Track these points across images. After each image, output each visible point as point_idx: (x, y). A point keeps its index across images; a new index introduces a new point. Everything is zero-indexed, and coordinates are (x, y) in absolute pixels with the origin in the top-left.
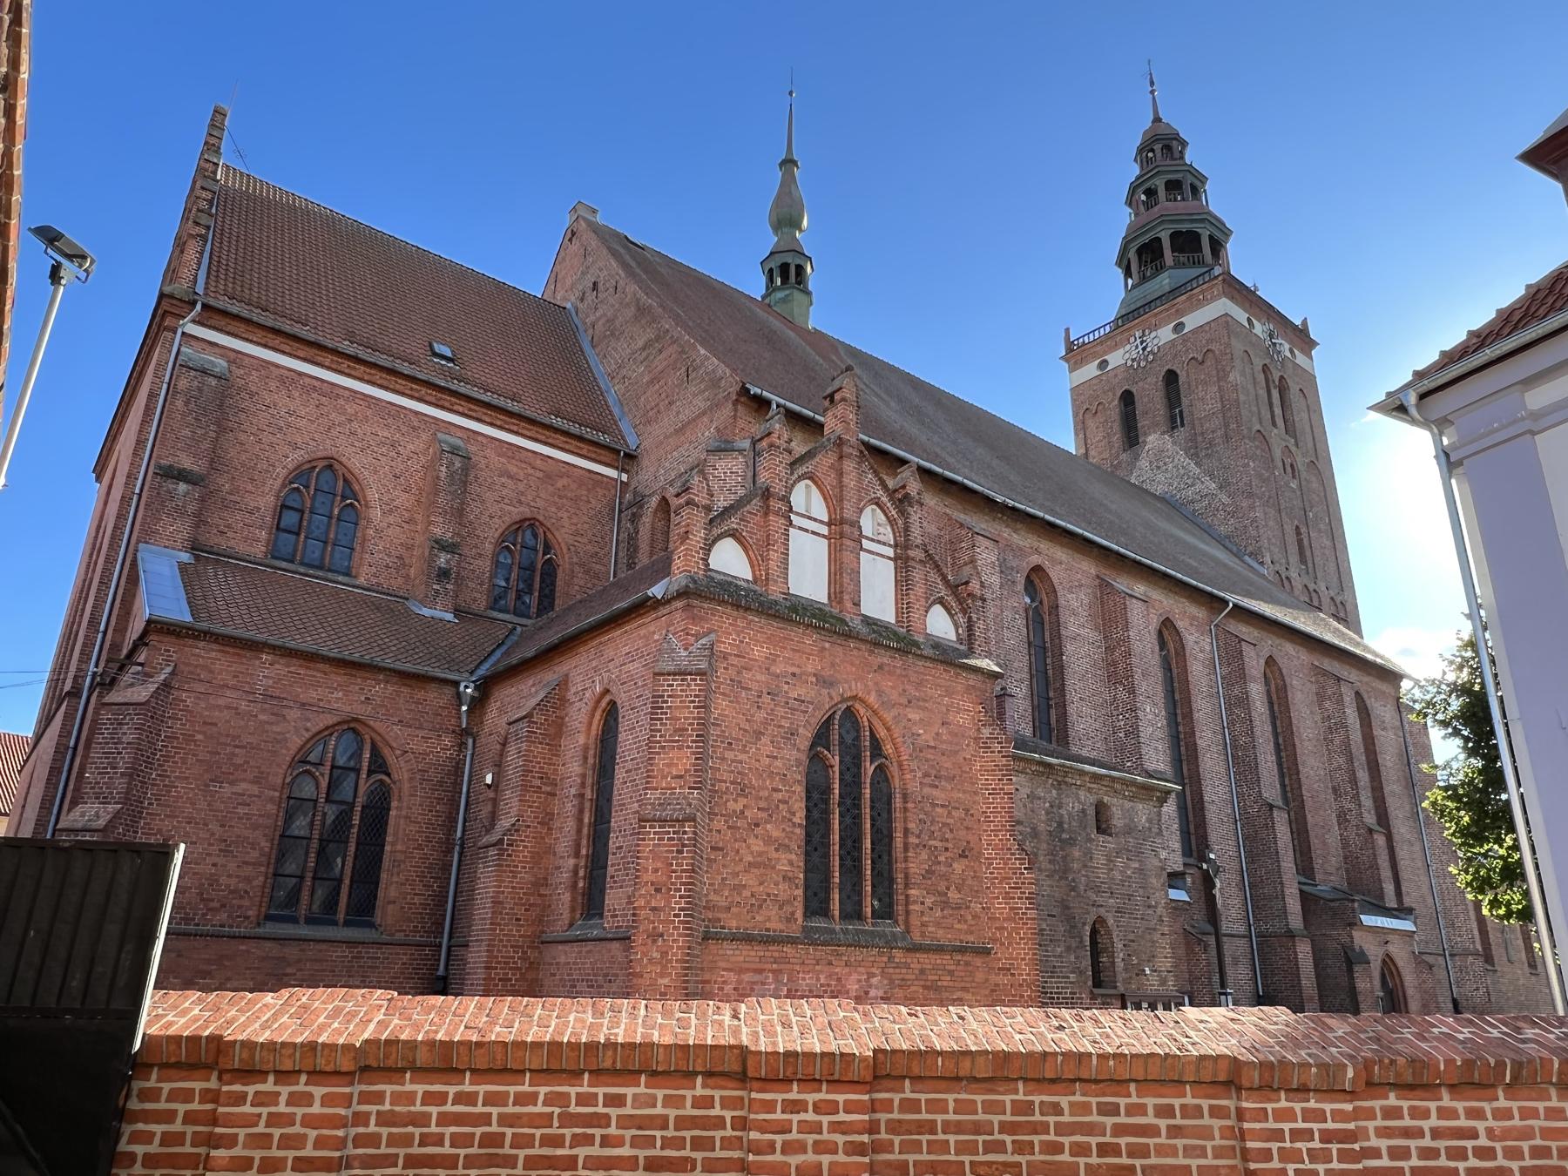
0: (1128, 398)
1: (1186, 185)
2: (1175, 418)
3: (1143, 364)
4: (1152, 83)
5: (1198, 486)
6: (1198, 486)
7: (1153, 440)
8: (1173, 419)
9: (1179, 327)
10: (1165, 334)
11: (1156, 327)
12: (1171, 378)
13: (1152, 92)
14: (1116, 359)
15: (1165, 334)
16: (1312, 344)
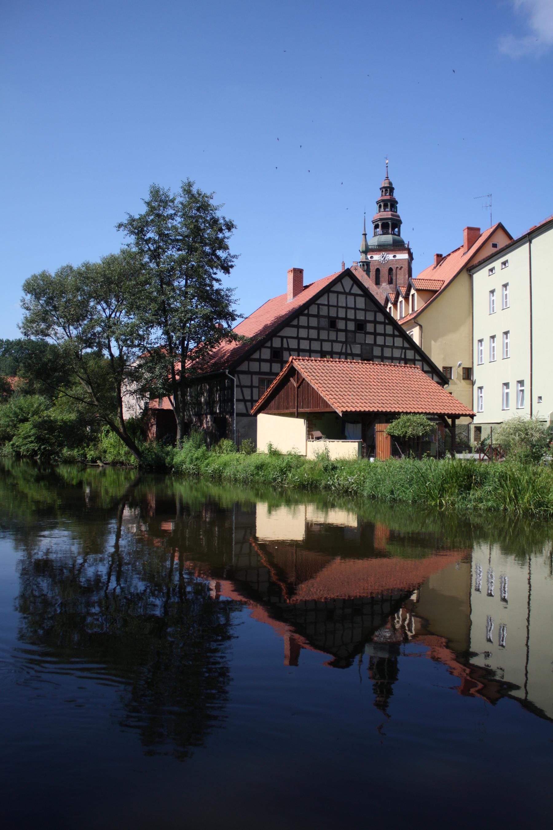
0: (378, 270)
9: (394, 256)
10: (390, 257)
11: (389, 254)
12: (391, 270)
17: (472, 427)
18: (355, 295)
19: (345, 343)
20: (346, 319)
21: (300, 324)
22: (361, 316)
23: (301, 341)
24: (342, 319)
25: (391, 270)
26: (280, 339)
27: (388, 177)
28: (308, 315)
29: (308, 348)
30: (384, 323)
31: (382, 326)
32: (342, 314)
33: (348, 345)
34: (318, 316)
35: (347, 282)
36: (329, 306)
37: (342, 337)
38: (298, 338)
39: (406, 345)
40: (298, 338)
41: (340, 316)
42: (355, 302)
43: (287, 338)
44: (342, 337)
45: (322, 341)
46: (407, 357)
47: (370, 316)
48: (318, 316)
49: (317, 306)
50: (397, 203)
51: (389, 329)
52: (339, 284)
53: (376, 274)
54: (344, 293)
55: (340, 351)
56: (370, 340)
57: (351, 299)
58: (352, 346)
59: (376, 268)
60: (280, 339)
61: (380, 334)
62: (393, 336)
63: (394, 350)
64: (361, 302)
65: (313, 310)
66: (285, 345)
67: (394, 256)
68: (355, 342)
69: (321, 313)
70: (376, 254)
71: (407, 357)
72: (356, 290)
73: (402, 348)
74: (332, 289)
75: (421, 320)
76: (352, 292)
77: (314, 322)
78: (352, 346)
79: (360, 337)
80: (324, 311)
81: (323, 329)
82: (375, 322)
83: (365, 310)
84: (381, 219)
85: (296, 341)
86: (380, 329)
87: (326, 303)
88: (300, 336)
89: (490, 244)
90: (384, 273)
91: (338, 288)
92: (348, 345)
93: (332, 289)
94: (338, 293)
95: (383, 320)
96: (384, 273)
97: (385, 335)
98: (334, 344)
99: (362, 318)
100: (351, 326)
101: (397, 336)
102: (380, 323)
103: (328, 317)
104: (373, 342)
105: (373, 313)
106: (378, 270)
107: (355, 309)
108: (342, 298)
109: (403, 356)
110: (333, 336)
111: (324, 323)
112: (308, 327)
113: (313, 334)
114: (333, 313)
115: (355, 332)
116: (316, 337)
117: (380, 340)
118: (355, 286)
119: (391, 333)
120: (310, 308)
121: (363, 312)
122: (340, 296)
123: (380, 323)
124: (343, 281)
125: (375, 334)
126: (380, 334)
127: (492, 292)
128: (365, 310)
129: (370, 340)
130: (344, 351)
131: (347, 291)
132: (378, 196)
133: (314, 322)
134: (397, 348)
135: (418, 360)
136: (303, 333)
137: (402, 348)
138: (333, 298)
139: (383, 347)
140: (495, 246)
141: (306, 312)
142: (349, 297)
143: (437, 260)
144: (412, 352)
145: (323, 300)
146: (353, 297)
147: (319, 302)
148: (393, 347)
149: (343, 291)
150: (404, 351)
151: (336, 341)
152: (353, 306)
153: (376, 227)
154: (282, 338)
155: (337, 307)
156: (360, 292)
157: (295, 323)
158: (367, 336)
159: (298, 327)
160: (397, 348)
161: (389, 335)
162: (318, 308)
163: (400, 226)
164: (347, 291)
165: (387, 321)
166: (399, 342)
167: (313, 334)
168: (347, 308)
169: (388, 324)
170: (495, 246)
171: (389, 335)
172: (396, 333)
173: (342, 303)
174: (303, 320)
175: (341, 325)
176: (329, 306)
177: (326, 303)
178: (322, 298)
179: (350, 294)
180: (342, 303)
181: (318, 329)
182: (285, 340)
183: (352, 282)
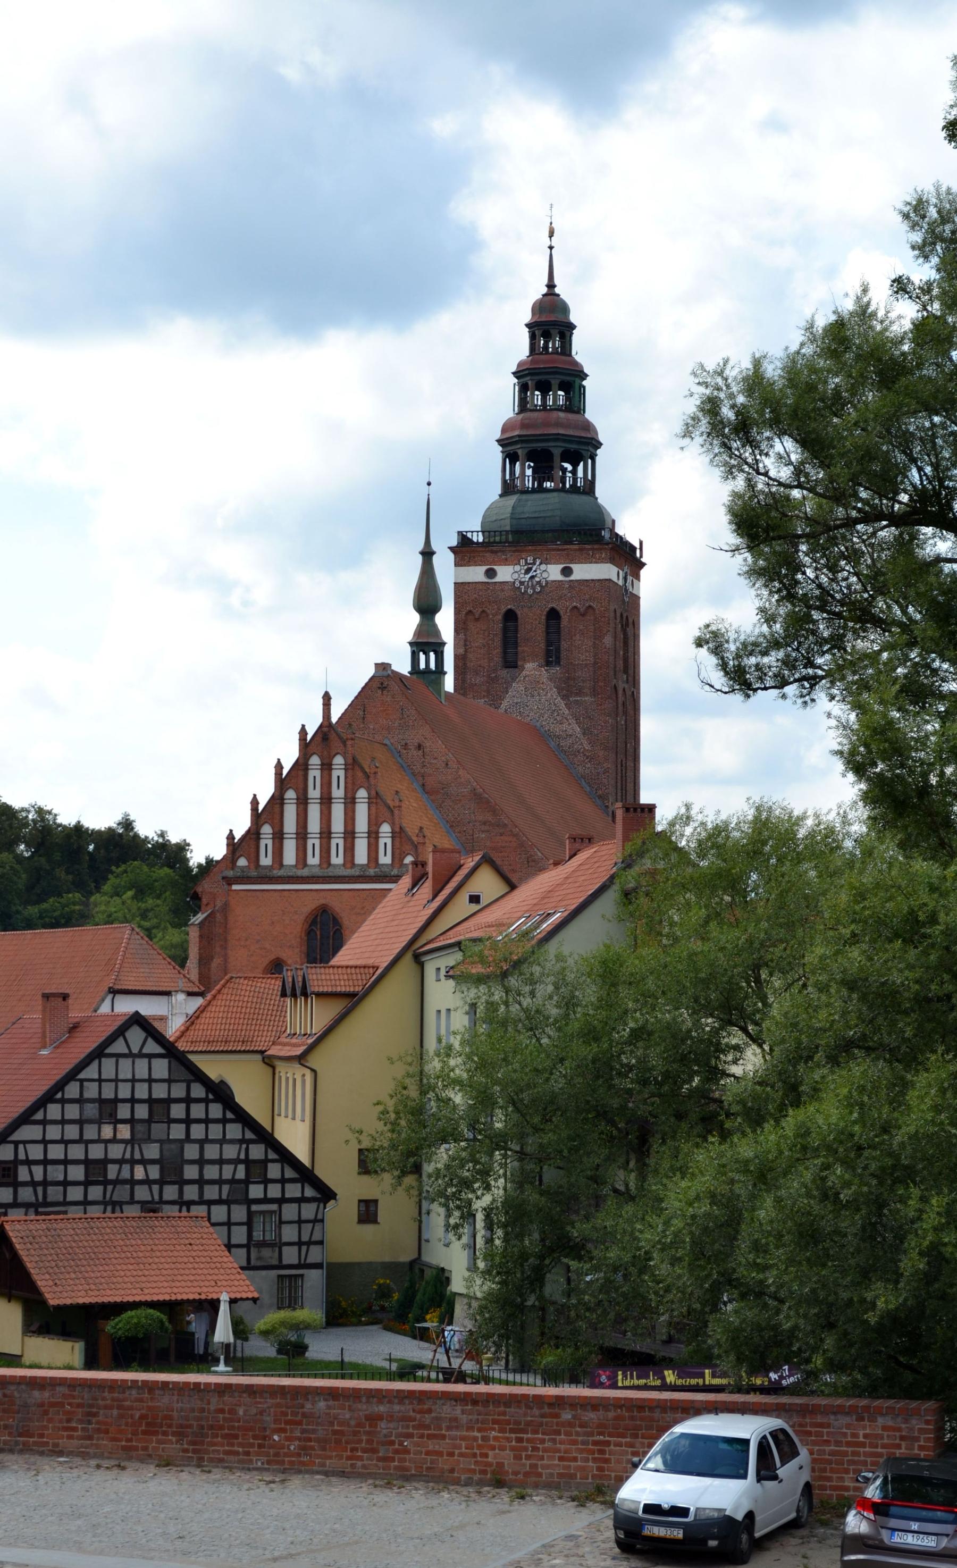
0: (510, 616)
1: (571, 380)
2: (552, 656)
3: (530, 591)
4: (551, 234)
5: (565, 726)
6: (565, 726)
7: (530, 668)
8: (548, 654)
9: (567, 571)
10: (553, 572)
11: (546, 561)
12: (553, 615)
13: (551, 248)
14: (505, 573)
15: (553, 572)
16: (643, 565)
17: (417, 1268)
18: (150, 1056)
19: (131, 1142)
20: (133, 1101)
21: (49, 1118)
22: (160, 1092)
23: (49, 1146)
24: (124, 1101)
25: (553, 615)
26: (12, 1146)
27: (551, 286)
28: (63, 1101)
29: (62, 1157)
30: (206, 1101)
31: (202, 1106)
32: (124, 1092)
33: (136, 1147)
34: (80, 1101)
35: (136, 1036)
36: (100, 1081)
37: (124, 1132)
38: (45, 1142)
39: (249, 1135)
40: (45, 1142)
41: (120, 1096)
42: (150, 1069)
43: (25, 1142)
44: (124, 1132)
45: (88, 1142)
46: (251, 1157)
47: (178, 1091)
48: (80, 1101)
49: (78, 1083)
50: (584, 376)
51: (216, 1110)
52: (121, 1040)
53: (505, 630)
54: (130, 1055)
55: (120, 1157)
56: (177, 1132)
57: (142, 1064)
58: (144, 1146)
59: (504, 609)
60: (12, 1146)
61: (198, 1121)
62: (224, 1121)
63: (225, 1146)
64: (161, 1068)
65: (72, 1090)
66: (22, 1156)
67: (567, 571)
68: (149, 1140)
69: (87, 1095)
70: (505, 562)
71: (251, 1157)
72: (152, 1047)
73: (241, 1141)
74: (108, 1051)
75: (315, 1060)
76: (145, 1051)
77: (72, 1111)
78: (144, 1146)
79: (158, 1130)
80: (91, 1091)
81: (90, 1121)
82: (188, 1100)
83: (169, 1081)
84: (522, 440)
85: (41, 1147)
86: (197, 1111)
87: (96, 1077)
88: (47, 1138)
89: (464, 896)
90: (532, 625)
91: (119, 1047)
92: (136, 1147)
93: (108, 1051)
94: (118, 1056)
95: (203, 1095)
96: (532, 625)
97: (207, 1121)
98: (110, 1146)
99: (164, 1095)
100: (142, 1112)
101: (231, 1121)
102: (198, 1101)
103: (101, 1101)
104: (183, 1137)
105: (184, 1085)
106: (510, 616)
107: (150, 1081)
108: (125, 1064)
109: (242, 1156)
110: (107, 1131)
111: (92, 1110)
112: (63, 1122)
113: (72, 1132)
114: (108, 1093)
115: (149, 1121)
116: (77, 1137)
117: (197, 1131)
118: (150, 1040)
119: (220, 1116)
120: (67, 1088)
121: (166, 1085)
122: (121, 1061)
123: (198, 1101)
124: (127, 1034)
125: (188, 1121)
126: (198, 1121)
127: (439, 1011)
128: (169, 1081)
129: (177, 1132)
130: (128, 1156)
131: (135, 1050)
132: (519, 348)
133: (72, 1111)
134: (232, 1142)
135: (273, 1161)
136: (53, 1132)
137: (241, 1141)
138: (108, 1067)
139: (202, 1143)
140: (475, 899)
141: (59, 1095)
142: (137, 1061)
143: (413, 876)
144: (262, 1147)
145: (91, 1072)
146: (146, 1060)
147: (82, 1076)
148: (223, 1141)
149: (127, 1051)
150: (244, 1146)
151: (114, 1140)
152: (146, 1077)
153: (511, 457)
154: (16, 1143)
155: (116, 1080)
156: (159, 1050)
157: (39, 1116)
158: (172, 1125)
159: (44, 1122)
160: (232, 1142)
161: (216, 1121)
162: (82, 1087)
163: (593, 458)
164: (135, 1050)
165: (211, 1096)
166: (234, 1131)
167: (72, 1132)
168: (133, 1081)
169: (213, 1101)
170: (475, 899)
171: (216, 1121)
172: (229, 1115)
173: (125, 1073)
174: (54, 1111)
175: (123, 1112)
176: (100, 1081)
177: (96, 1077)
178: (88, 1069)
179: (141, 1055)
180: (125, 1073)
181: (81, 1122)
182: (21, 1147)
183: (143, 1035)
